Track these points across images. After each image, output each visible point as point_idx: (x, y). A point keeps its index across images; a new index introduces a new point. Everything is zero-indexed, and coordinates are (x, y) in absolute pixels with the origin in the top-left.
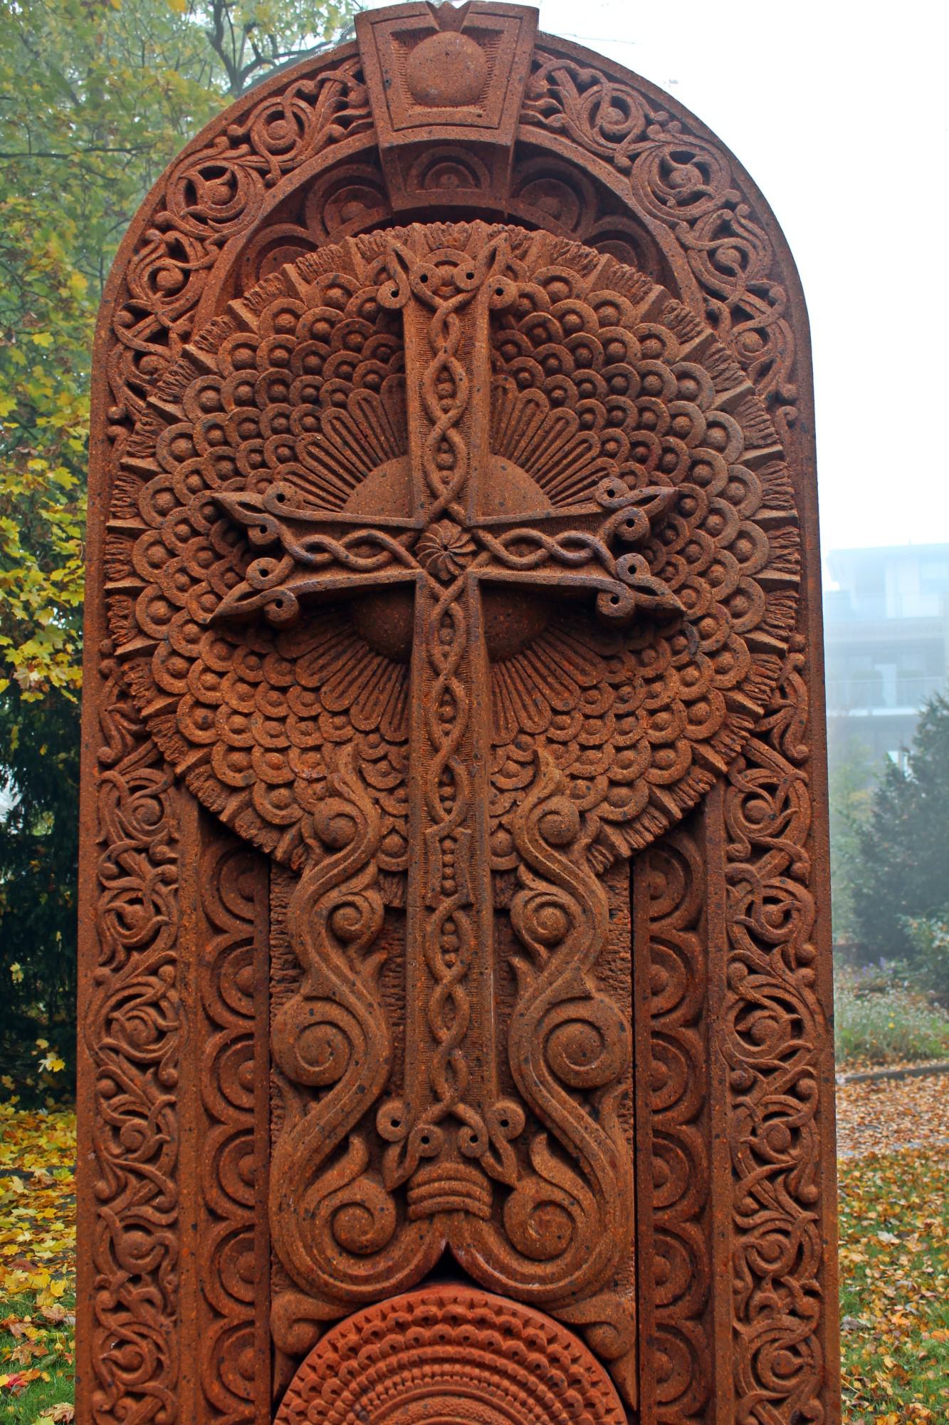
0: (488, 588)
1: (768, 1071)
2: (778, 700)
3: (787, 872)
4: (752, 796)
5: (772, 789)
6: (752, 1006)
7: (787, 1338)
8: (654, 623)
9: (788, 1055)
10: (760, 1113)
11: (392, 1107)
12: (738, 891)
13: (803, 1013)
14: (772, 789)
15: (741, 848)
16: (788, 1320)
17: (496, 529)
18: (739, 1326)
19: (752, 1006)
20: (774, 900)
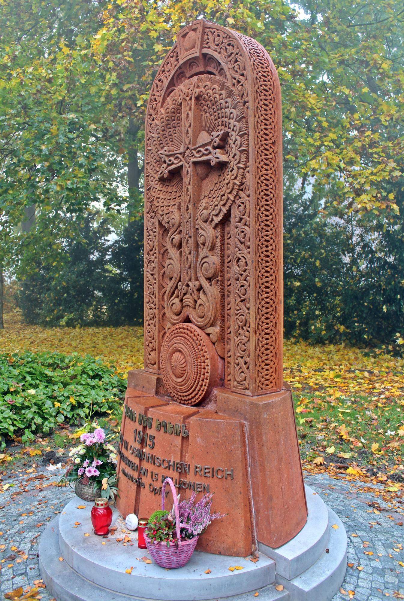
0: (195, 163)
1: (242, 275)
2: (244, 181)
3: (245, 225)
4: (240, 206)
5: (243, 203)
6: (239, 259)
7: (243, 342)
8: (222, 166)
9: (244, 271)
10: (240, 285)
11: (180, 283)
12: (237, 230)
13: (247, 261)
14: (243, 203)
15: (238, 219)
16: (244, 338)
17: (195, 149)
18: (235, 338)
19: (239, 259)
20: (243, 232)
